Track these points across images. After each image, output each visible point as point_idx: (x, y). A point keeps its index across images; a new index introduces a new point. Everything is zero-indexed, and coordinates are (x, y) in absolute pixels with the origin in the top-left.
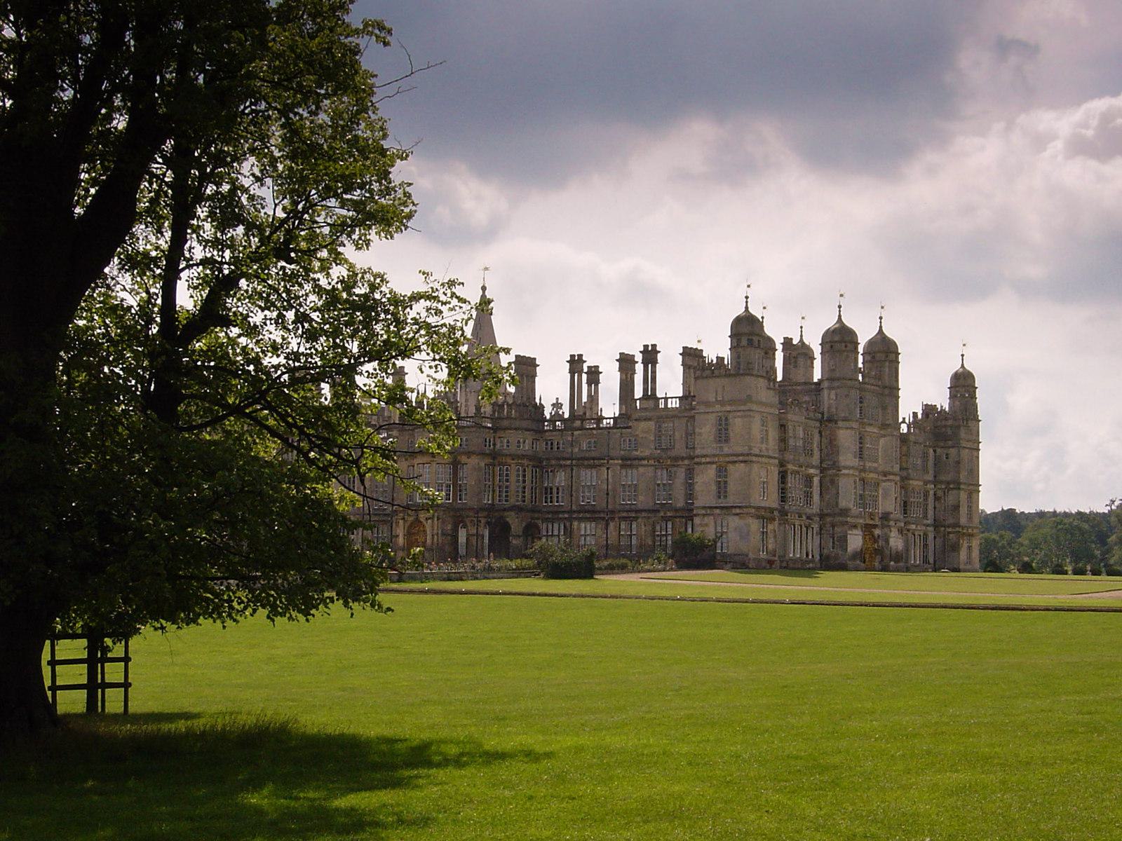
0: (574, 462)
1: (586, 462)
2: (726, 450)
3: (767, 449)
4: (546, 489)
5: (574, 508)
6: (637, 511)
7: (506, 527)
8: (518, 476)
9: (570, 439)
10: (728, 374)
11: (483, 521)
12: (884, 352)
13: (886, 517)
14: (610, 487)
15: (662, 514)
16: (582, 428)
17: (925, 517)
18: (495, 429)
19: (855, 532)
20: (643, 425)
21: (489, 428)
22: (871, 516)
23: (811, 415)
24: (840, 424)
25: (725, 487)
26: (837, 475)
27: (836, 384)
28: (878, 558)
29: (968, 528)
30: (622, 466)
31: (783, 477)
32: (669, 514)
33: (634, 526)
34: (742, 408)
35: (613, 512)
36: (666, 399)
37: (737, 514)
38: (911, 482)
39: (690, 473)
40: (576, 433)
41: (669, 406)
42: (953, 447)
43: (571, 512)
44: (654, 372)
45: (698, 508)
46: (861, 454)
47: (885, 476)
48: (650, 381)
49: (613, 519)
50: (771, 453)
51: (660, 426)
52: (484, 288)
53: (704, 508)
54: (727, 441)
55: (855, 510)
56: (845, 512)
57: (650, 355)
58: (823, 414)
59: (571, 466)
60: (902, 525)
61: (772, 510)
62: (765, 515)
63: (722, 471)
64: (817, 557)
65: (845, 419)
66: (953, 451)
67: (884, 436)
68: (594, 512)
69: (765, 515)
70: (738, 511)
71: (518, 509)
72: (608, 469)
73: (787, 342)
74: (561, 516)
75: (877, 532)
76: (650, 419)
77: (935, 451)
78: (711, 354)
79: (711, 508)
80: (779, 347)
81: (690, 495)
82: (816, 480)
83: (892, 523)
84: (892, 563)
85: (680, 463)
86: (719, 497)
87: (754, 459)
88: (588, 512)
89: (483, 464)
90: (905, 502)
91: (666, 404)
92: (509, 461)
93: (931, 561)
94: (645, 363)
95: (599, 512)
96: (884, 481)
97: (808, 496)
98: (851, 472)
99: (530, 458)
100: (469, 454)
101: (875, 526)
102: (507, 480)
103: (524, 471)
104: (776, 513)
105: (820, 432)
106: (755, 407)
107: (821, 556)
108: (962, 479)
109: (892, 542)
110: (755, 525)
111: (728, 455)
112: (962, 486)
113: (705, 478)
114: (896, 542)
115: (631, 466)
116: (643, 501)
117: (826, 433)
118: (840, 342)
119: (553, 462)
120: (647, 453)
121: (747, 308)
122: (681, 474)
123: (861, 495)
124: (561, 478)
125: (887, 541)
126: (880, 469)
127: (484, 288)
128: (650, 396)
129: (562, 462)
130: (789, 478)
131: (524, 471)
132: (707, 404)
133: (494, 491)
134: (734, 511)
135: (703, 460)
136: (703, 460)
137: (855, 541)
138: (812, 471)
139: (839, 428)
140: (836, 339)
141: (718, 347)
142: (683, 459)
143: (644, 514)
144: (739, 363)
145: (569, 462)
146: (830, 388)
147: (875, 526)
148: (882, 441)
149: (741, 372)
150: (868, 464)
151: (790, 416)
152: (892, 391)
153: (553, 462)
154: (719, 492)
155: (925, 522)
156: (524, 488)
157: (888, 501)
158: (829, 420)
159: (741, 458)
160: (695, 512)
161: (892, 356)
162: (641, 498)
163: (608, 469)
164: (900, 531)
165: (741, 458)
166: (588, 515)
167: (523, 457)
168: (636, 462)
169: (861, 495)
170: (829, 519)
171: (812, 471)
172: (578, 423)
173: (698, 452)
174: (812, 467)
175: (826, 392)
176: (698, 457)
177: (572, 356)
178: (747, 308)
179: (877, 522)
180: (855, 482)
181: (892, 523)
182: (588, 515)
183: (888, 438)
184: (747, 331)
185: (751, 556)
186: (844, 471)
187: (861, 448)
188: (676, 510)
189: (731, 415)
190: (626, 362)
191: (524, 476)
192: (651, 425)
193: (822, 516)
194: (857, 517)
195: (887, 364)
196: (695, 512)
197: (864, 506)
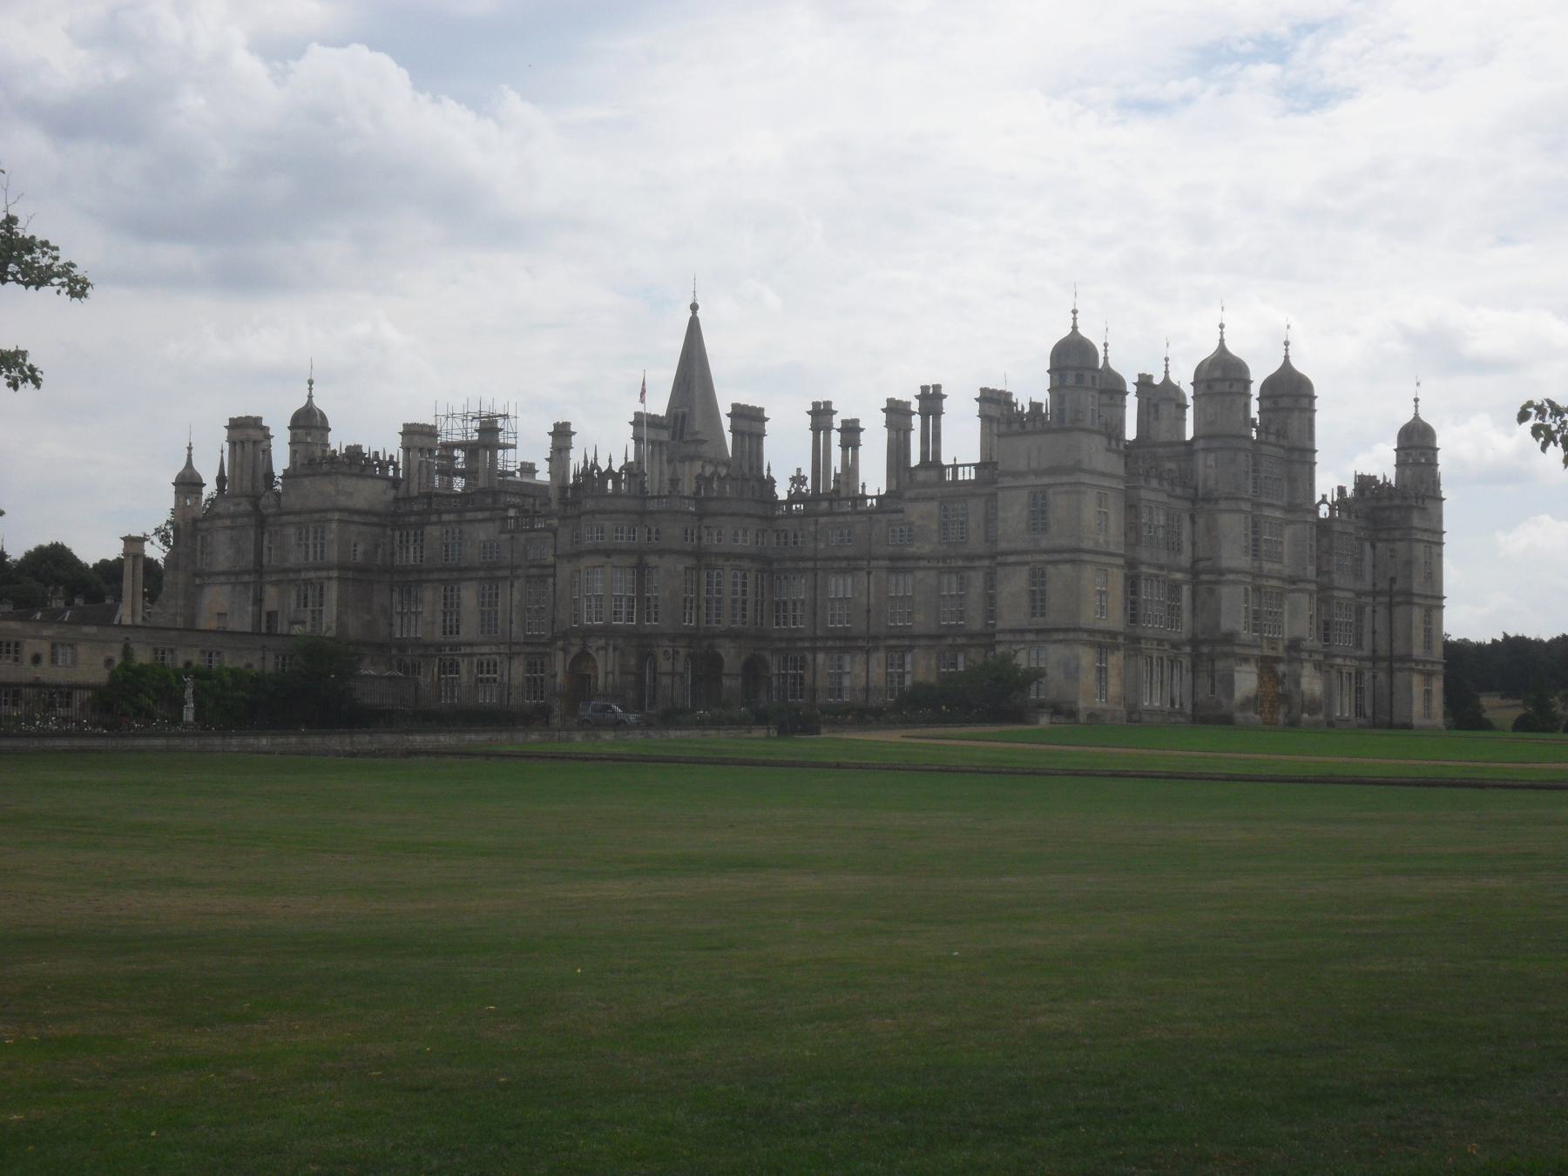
0: (819, 564)
1: (836, 565)
2: (1044, 544)
3: (1107, 542)
4: (778, 604)
5: (819, 633)
6: (914, 637)
7: (716, 661)
8: (735, 584)
9: (812, 528)
10: (1048, 430)
11: (683, 652)
12: (1291, 393)
13: (1294, 645)
14: (872, 600)
15: (950, 641)
16: (830, 513)
17: (1359, 645)
18: (700, 516)
19: (1245, 668)
20: (922, 507)
21: (692, 514)
22: (1273, 643)
23: (1178, 491)
24: (1223, 505)
25: (1043, 600)
26: (1218, 582)
27: (1216, 444)
28: (1283, 710)
29: (1425, 662)
30: (891, 570)
31: (1132, 584)
32: (960, 641)
33: (908, 659)
34: (1065, 479)
35: (875, 638)
36: (955, 467)
37: (1061, 641)
38: (1336, 593)
39: (991, 582)
40: (822, 520)
41: (960, 478)
42: (1401, 540)
43: (814, 639)
44: (937, 427)
45: (1003, 631)
46: (1255, 551)
47: (1294, 582)
48: (932, 438)
49: (876, 648)
50: (1112, 549)
51: (945, 509)
52: (694, 307)
53: (1012, 631)
54: (1045, 529)
55: (1245, 635)
56: (1230, 638)
57: (932, 400)
58: (1196, 489)
59: (814, 570)
60: (1321, 657)
61: (1113, 635)
62: (1104, 643)
63: (1038, 578)
64: (1188, 709)
66: (1401, 547)
68: (846, 638)
69: (1104, 643)
70: (1061, 636)
72: (869, 573)
73: (1144, 382)
74: (799, 644)
75: (1281, 668)
76: (932, 499)
77: (1373, 547)
78: (1022, 402)
79: (1022, 631)
80: (1131, 389)
81: (991, 613)
82: (1186, 590)
83: (1305, 655)
84: (1305, 716)
85: (977, 563)
86: (1033, 615)
87: (1086, 557)
88: (840, 638)
89: (681, 567)
90: (1327, 624)
91: (955, 474)
92: (720, 562)
93: (1369, 711)
94: (924, 414)
95: (856, 638)
96: (1293, 591)
97: (1174, 611)
98: (1240, 577)
99: (753, 558)
100: (661, 553)
101: (1278, 660)
102: (719, 592)
103: (744, 577)
104: (1121, 640)
105: (1192, 518)
106: (1086, 479)
107: (1194, 705)
108: (1416, 588)
109: (1306, 684)
110: (1087, 657)
111: (1046, 552)
112: (1416, 600)
113: (1014, 585)
114: (1311, 683)
115: (905, 571)
116: (922, 621)
117: (1201, 522)
118: (1223, 380)
119: (788, 564)
120: (927, 549)
121: (1075, 328)
122: (977, 580)
123: (1255, 612)
124: (800, 589)
125: (1298, 683)
126: (1287, 572)
127: (694, 307)
128: (932, 462)
129: (801, 565)
131: (744, 577)
132: (1016, 475)
133: (699, 607)
134: (1056, 636)
135: (1012, 559)
136: (1012, 559)
137: (1246, 681)
138: (1179, 576)
139: (1221, 511)
140: (1217, 374)
141: (1031, 386)
142: (980, 557)
143: (923, 642)
144: (1062, 411)
145: (810, 564)
146: (1207, 450)
148: (1288, 531)
149: (1067, 424)
150: (1267, 566)
151: (1144, 494)
152: (1301, 456)
153: (788, 564)
154: (1034, 608)
155: (1359, 653)
156: (744, 602)
157: (1298, 619)
158: (1207, 499)
159: (1066, 556)
160: (998, 637)
161: (1304, 402)
162: (919, 617)
163: (869, 573)
164: (1318, 666)
165: (1066, 556)
166: (838, 644)
167: (740, 557)
168: (911, 564)
169: (1255, 612)
170: (1205, 649)
171: (1179, 576)
172: (824, 505)
173: (1003, 546)
174: (1180, 570)
175: (1201, 457)
176: (1003, 554)
177: (816, 405)
178: (1075, 328)
179: (1281, 652)
180: (1246, 594)
181: (1305, 655)
182: (838, 644)
184: (1074, 361)
185: (1082, 704)
186: (1231, 577)
187: (1255, 540)
188: (971, 636)
189: (1051, 491)
190: (896, 413)
191: (744, 585)
192: (934, 506)
193: (1195, 642)
194: (1249, 646)
195: (1297, 414)
196: (998, 637)
197: (1257, 628)
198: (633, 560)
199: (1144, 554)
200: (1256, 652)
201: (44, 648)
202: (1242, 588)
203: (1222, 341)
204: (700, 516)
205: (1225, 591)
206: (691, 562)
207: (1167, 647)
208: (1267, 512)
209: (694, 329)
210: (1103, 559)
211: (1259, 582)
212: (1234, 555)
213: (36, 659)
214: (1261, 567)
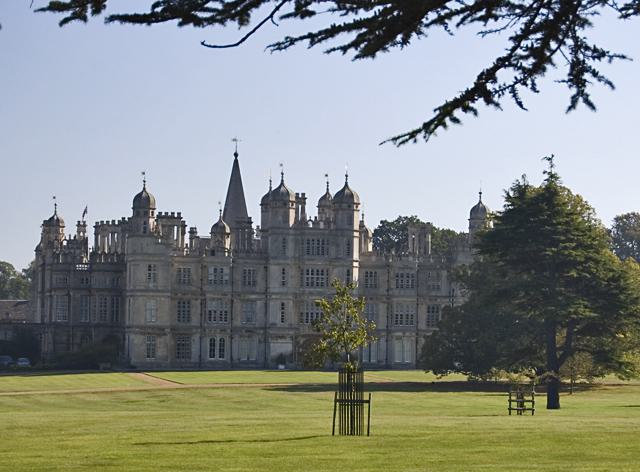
24: (271, 261)
38: (395, 299)
52: (236, 155)
65: (275, 258)
67: (336, 266)
71: (97, 326)
82: (260, 304)
87: (139, 294)
98: (278, 297)
127: (236, 155)
130: (209, 303)
138: (253, 297)
148: (336, 271)
167: (102, 290)
183: (341, 269)
186: (273, 297)
193: (265, 328)
199: (205, 288)
200: (292, 333)
202: (279, 303)
203: (282, 181)
205: (271, 303)
206: (84, 293)
207: (244, 331)
209: (236, 162)
210: (151, 294)
212: (275, 286)
214: (303, 293)
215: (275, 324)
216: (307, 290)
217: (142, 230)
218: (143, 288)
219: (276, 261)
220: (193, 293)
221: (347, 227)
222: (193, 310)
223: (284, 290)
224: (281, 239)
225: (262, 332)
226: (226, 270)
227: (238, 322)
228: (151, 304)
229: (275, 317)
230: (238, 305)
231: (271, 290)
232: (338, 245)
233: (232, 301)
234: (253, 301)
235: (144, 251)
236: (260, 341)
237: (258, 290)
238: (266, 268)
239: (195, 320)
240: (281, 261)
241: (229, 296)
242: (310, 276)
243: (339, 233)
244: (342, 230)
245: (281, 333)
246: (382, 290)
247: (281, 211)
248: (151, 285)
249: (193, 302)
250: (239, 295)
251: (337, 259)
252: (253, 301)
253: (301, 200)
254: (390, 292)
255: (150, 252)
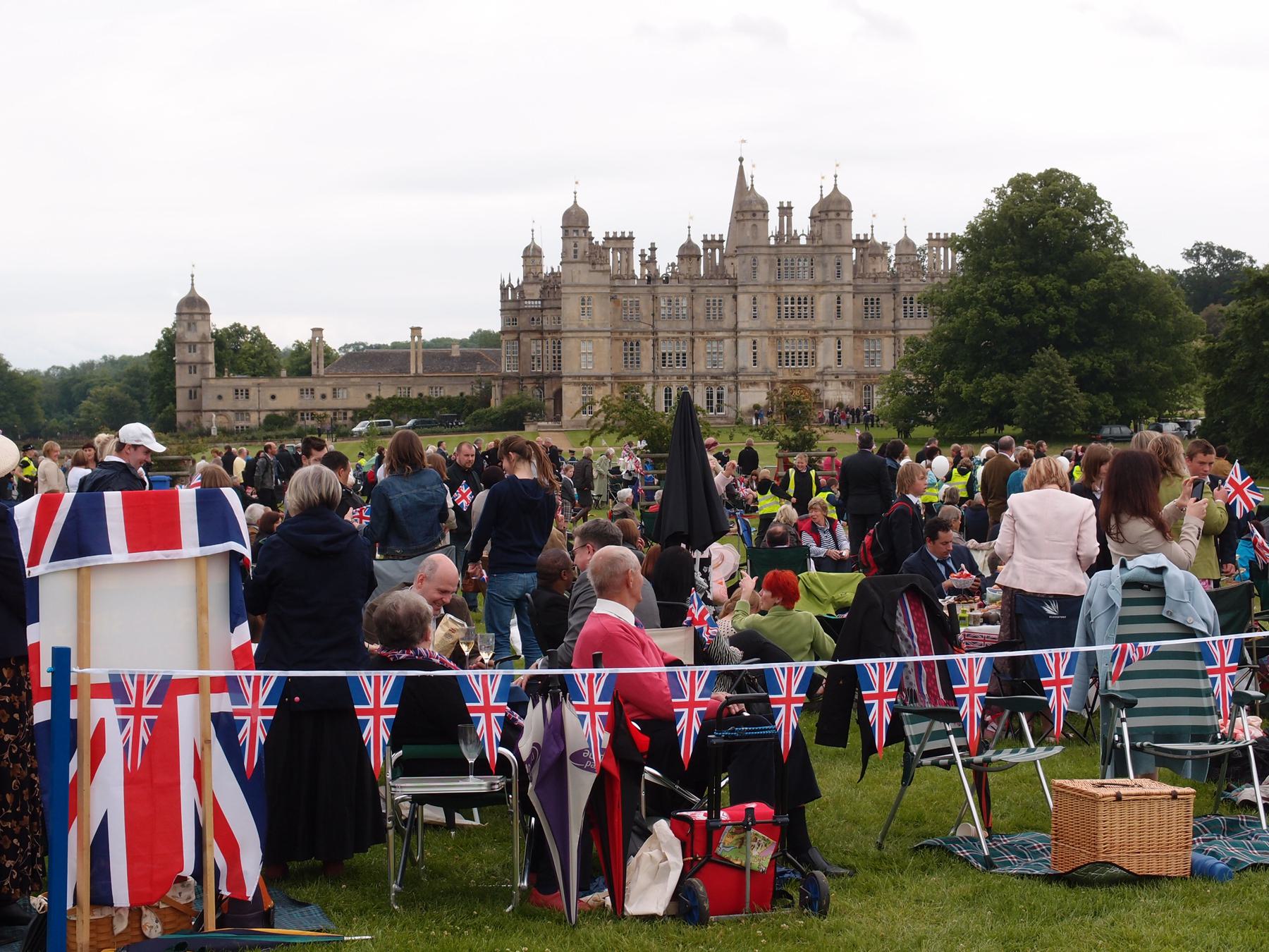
24: (739, 289)
38: (902, 333)
50: (597, 327)
61: (602, 378)
67: (823, 293)
75: (813, 387)
82: (728, 343)
83: (826, 378)
87: (569, 335)
92: (547, 336)
147: (811, 381)
148: (824, 297)
161: (843, 215)
179: (806, 376)
181: (826, 378)
186: (743, 334)
193: (735, 374)
198: (515, 336)
199: (660, 325)
200: (766, 378)
201: (329, 392)
202: (749, 341)
204: (542, 310)
205: (741, 342)
208: (785, 289)
210: (585, 334)
211: (780, 334)
212: (745, 322)
213: (324, 397)
214: (781, 326)
215: (744, 368)
216: (787, 324)
217: (572, 254)
218: (575, 327)
219: (744, 289)
220: (643, 332)
221: (835, 242)
222: (643, 353)
223: (756, 324)
224: (749, 259)
225: (732, 378)
226: (684, 303)
227: (701, 367)
228: (586, 347)
229: (745, 360)
230: (699, 344)
231: (740, 326)
232: (825, 266)
233: (693, 340)
234: (720, 340)
235: (576, 281)
236: (729, 391)
237: (725, 326)
238: (735, 297)
239: (646, 366)
240: (751, 289)
241: (688, 334)
242: (789, 305)
243: (826, 250)
244: (830, 246)
245: (754, 379)
246: (887, 321)
247: (749, 224)
248: (585, 324)
249: (643, 343)
250: (702, 333)
251: (825, 284)
252: (720, 340)
253: (786, 211)
254: (897, 324)
255: (583, 281)
